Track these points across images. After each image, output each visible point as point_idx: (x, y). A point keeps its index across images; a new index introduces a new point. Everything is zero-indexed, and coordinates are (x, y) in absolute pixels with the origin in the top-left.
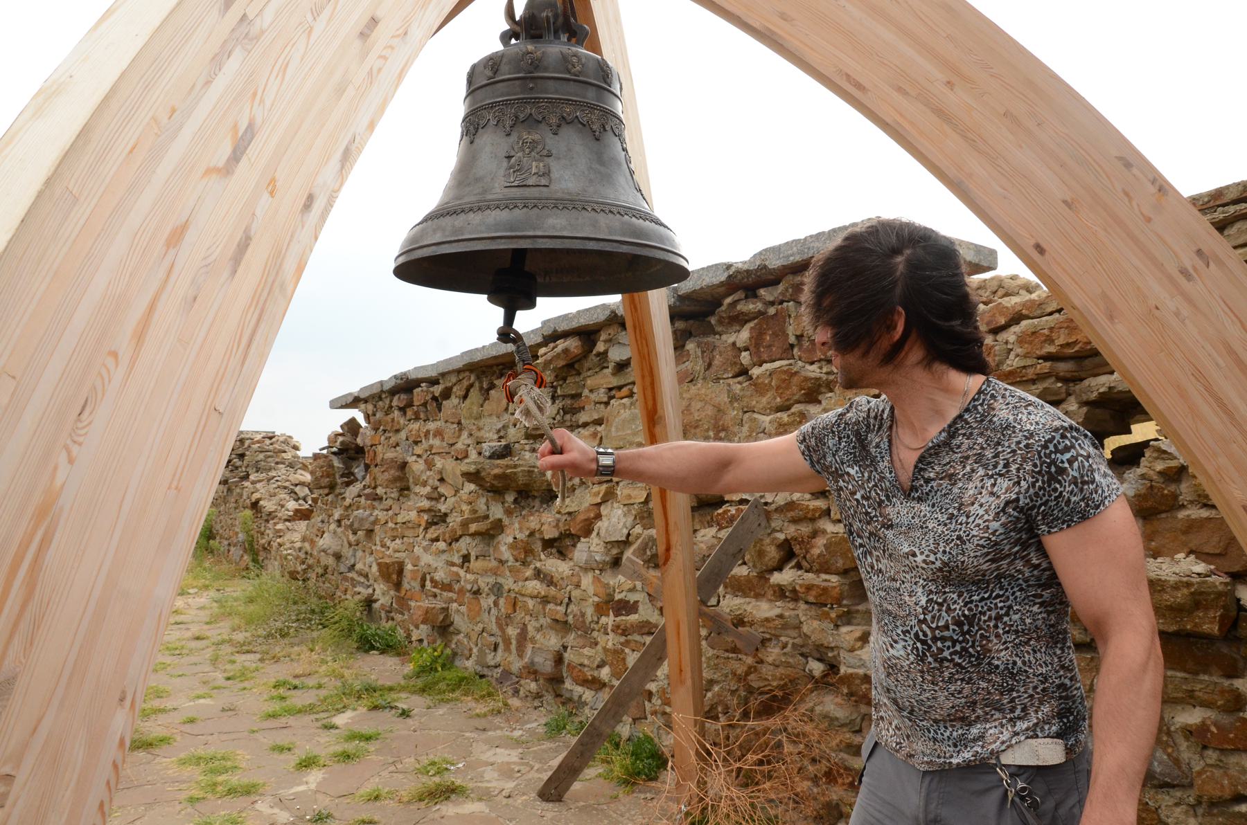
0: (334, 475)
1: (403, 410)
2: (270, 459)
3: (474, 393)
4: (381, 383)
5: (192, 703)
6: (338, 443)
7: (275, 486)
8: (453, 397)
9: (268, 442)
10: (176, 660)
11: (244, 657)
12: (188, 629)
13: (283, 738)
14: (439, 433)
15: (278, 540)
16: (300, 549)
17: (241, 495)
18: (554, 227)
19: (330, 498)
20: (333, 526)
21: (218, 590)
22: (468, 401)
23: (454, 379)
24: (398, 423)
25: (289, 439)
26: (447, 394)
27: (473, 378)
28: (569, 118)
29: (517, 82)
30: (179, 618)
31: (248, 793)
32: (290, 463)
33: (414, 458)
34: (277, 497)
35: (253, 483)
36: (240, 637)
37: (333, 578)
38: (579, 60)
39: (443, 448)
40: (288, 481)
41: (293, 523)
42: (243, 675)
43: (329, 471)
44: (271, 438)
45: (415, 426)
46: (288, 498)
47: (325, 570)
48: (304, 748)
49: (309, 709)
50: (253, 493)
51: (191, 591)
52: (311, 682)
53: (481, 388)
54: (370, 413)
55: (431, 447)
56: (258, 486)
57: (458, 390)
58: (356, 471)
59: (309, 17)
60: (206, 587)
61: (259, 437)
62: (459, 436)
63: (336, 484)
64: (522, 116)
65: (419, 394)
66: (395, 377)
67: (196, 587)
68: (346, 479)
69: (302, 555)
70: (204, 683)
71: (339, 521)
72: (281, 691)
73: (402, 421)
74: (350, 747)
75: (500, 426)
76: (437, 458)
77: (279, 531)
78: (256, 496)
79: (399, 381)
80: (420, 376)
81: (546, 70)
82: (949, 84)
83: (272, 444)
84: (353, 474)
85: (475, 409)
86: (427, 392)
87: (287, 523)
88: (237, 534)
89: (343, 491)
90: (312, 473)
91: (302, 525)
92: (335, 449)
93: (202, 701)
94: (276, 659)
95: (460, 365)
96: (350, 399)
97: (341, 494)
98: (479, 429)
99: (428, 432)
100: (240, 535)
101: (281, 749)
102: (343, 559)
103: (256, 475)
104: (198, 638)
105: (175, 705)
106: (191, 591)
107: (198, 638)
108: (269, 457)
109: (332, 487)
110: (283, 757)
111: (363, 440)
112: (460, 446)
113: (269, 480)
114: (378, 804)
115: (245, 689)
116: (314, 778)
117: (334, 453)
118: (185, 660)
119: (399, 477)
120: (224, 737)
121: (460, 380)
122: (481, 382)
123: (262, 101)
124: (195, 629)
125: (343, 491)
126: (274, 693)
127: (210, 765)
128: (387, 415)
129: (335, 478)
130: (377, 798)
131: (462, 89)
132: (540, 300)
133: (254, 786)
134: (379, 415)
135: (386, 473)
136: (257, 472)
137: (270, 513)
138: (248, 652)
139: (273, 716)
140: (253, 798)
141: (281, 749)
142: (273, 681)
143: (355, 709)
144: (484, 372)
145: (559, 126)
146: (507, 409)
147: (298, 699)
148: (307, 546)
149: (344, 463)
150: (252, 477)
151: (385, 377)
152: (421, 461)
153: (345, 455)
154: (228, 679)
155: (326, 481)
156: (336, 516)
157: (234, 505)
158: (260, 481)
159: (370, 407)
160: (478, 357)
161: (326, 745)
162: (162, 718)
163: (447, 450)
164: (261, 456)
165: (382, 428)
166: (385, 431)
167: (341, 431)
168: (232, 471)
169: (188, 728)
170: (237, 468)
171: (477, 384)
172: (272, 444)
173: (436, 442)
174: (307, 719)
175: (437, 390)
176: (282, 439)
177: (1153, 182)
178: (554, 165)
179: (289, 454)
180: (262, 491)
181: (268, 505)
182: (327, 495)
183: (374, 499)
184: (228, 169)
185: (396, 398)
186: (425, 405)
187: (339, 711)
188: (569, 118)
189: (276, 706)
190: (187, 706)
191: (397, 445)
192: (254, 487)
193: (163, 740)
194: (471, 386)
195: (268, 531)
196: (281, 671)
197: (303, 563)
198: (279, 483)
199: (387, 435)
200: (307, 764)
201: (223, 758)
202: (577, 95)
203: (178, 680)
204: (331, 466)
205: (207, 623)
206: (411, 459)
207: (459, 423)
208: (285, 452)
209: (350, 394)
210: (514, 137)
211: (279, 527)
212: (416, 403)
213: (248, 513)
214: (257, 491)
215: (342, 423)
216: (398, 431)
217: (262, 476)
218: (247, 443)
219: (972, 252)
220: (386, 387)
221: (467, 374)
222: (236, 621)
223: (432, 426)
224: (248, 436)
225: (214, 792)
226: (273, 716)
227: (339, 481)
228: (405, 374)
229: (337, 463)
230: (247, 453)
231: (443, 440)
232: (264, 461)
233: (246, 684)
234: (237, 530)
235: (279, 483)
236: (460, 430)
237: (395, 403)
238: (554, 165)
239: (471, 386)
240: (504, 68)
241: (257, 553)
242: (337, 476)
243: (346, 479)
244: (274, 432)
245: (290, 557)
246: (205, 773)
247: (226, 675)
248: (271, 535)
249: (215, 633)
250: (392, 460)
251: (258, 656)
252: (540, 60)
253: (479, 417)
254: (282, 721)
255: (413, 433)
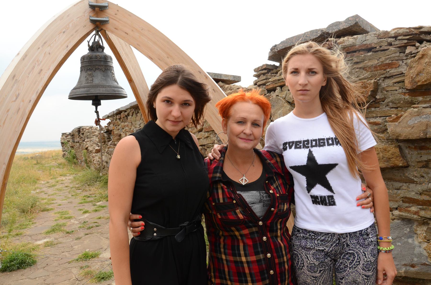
0: (105, 139)
1: (120, 119)
2: (91, 135)
3: (134, 114)
4: (113, 112)
5: (61, 202)
6: (106, 129)
7: (92, 143)
8: (130, 115)
9: (90, 129)
10: (59, 192)
11: (78, 191)
12: (64, 185)
13: (81, 208)
14: (127, 126)
15: (93, 159)
16: (98, 161)
17: (83, 146)
18: (91, 91)
19: (105, 145)
20: (106, 154)
21: (76, 174)
22: (133, 116)
23: (129, 110)
24: (119, 123)
25: (97, 128)
26: (128, 115)
27: (134, 110)
28: (97, 68)
29: (87, 62)
30: (62, 182)
31: (69, 218)
32: (97, 136)
33: (123, 133)
34: (93, 146)
35: (86, 142)
36: (77, 186)
37: (106, 169)
38: (99, 56)
39: (128, 130)
40: (96, 141)
41: (98, 154)
42: (76, 195)
43: (103, 138)
44: (91, 128)
45: (123, 124)
46: (96, 146)
47: (104, 167)
48: (86, 209)
49: (91, 202)
50: (86, 145)
51: (68, 175)
52: (93, 196)
53: (136, 113)
54: (112, 120)
55: (126, 130)
56: (88, 143)
57: (131, 114)
58: (111, 137)
59: (28, 75)
60: (72, 174)
61: (88, 128)
62: (132, 127)
63: (106, 141)
64: (88, 68)
65: (122, 114)
66: (116, 110)
67: (69, 174)
68: (108, 140)
69: (99, 163)
70: (65, 197)
71: (107, 152)
72: (85, 198)
73: (120, 122)
74: (97, 209)
75: (139, 123)
76: (127, 133)
77: (93, 156)
78: (87, 146)
79: (117, 111)
80: (122, 110)
81: (92, 59)
82: (168, 57)
83: (91, 130)
84: (110, 138)
85: (135, 119)
86: (124, 114)
87: (96, 154)
88: (83, 158)
89: (108, 143)
90: (98, 138)
91: (99, 154)
92: (104, 131)
93: (64, 201)
94: (86, 191)
95: (129, 107)
96: (107, 116)
97: (107, 144)
98: (136, 124)
99: (125, 125)
100: (83, 158)
101: (81, 210)
102: (108, 163)
103: (87, 139)
104: (66, 187)
105: (56, 202)
106: (68, 175)
107: (66, 187)
108: (91, 134)
109: (105, 142)
110: (80, 211)
111: (111, 128)
112: (132, 129)
113: (91, 141)
114: (100, 219)
115: (76, 198)
116: (86, 215)
117: (105, 132)
118: (62, 192)
119: (119, 138)
120: (67, 208)
121: (131, 111)
122: (136, 111)
123: (20, 90)
124: (66, 185)
125: (108, 143)
126: (83, 198)
127: (62, 213)
128: (116, 121)
129: (105, 139)
130: (100, 218)
131: (80, 62)
132: (102, 102)
133: (71, 217)
134: (114, 121)
135: (115, 138)
136: (88, 139)
137: (91, 151)
138: (79, 189)
139: (81, 203)
140: (70, 219)
141: (81, 210)
142: (83, 196)
143: (102, 201)
144: (136, 109)
145: (95, 70)
146: (141, 119)
147: (89, 199)
148: (100, 160)
149: (108, 135)
150: (86, 140)
151: (114, 110)
152: (124, 134)
153: (108, 133)
154: (72, 196)
155: (103, 141)
156: (106, 151)
157: (81, 149)
158: (88, 141)
159: (112, 118)
160: (133, 105)
161: (91, 208)
162: (52, 205)
163: (129, 130)
164: (88, 134)
165: (115, 125)
166: (116, 125)
167: (107, 126)
168: (80, 139)
169: (59, 207)
170: (82, 138)
171: (135, 112)
172: (91, 130)
173: (127, 128)
174: (91, 204)
175: (126, 113)
176: (94, 128)
177: (205, 76)
178: (94, 78)
179: (97, 133)
180: (89, 144)
181: (90, 149)
182: (104, 145)
183: (114, 145)
184: (15, 101)
185: (118, 115)
186: (124, 118)
187: (98, 202)
188: (97, 68)
189: (82, 201)
190: (60, 202)
191: (119, 129)
192: (87, 143)
193: (51, 209)
194: (133, 112)
195: (91, 157)
196: (87, 194)
197: (99, 165)
198: (94, 142)
199: (116, 126)
200: (86, 212)
201: (65, 212)
202: (99, 63)
203: (59, 197)
204: (104, 136)
205: (70, 183)
206: (122, 133)
207: (132, 123)
208: (95, 132)
209: (107, 115)
210: (87, 73)
211: (93, 155)
212: (122, 117)
213: (85, 151)
214: (87, 144)
215: (107, 123)
216: (119, 125)
217: (89, 140)
218: (84, 130)
219: (232, 78)
220: (115, 113)
221: (132, 109)
222: (78, 182)
223: (126, 124)
224: (84, 128)
225: (61, 218)
226: (81, 203)
227: (106, 140)
228: (119, 109)
229: (106, 135)
230: (84, 133)
231: (128, 128)
232: (89, 135)
233: (77, 197)
234: (83, 157)
235: (94, 142)
236: (132, 125)
237: (117, 117)
238: (94, 78)
239: (133, 112)
240: (85, 59)
241: (88, 163)
242: (106, 139)
243: (108, 140)
244: (93, 126)
245: (96, 164)
246: (60, 215)
247: (71, 195)
248: (91, 158)
249: (71, 186)
250: (117, 134)
251: (82, 190)
252: (91, 57)
253: (135, 121)
254: (84, 204)
255: (122, 126)
